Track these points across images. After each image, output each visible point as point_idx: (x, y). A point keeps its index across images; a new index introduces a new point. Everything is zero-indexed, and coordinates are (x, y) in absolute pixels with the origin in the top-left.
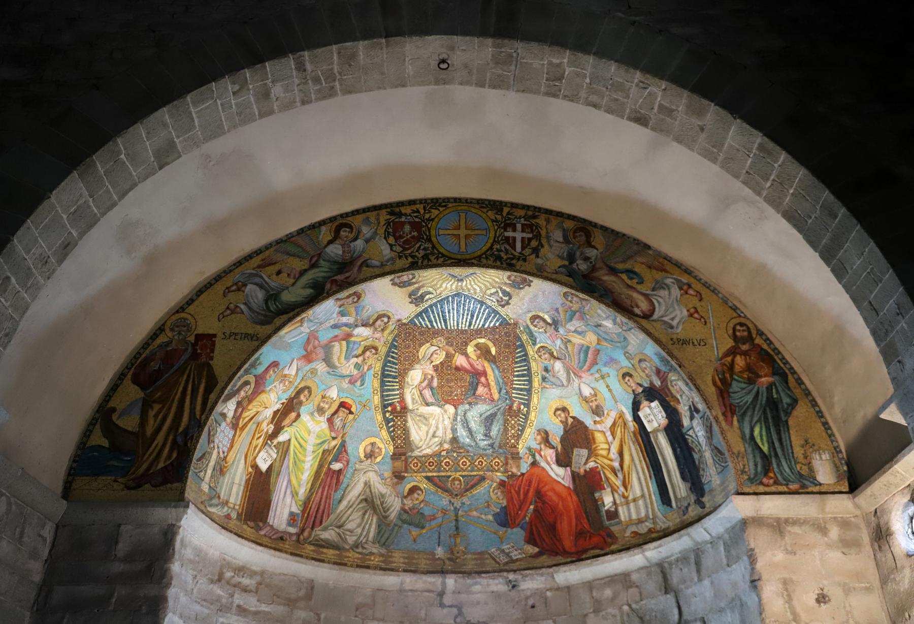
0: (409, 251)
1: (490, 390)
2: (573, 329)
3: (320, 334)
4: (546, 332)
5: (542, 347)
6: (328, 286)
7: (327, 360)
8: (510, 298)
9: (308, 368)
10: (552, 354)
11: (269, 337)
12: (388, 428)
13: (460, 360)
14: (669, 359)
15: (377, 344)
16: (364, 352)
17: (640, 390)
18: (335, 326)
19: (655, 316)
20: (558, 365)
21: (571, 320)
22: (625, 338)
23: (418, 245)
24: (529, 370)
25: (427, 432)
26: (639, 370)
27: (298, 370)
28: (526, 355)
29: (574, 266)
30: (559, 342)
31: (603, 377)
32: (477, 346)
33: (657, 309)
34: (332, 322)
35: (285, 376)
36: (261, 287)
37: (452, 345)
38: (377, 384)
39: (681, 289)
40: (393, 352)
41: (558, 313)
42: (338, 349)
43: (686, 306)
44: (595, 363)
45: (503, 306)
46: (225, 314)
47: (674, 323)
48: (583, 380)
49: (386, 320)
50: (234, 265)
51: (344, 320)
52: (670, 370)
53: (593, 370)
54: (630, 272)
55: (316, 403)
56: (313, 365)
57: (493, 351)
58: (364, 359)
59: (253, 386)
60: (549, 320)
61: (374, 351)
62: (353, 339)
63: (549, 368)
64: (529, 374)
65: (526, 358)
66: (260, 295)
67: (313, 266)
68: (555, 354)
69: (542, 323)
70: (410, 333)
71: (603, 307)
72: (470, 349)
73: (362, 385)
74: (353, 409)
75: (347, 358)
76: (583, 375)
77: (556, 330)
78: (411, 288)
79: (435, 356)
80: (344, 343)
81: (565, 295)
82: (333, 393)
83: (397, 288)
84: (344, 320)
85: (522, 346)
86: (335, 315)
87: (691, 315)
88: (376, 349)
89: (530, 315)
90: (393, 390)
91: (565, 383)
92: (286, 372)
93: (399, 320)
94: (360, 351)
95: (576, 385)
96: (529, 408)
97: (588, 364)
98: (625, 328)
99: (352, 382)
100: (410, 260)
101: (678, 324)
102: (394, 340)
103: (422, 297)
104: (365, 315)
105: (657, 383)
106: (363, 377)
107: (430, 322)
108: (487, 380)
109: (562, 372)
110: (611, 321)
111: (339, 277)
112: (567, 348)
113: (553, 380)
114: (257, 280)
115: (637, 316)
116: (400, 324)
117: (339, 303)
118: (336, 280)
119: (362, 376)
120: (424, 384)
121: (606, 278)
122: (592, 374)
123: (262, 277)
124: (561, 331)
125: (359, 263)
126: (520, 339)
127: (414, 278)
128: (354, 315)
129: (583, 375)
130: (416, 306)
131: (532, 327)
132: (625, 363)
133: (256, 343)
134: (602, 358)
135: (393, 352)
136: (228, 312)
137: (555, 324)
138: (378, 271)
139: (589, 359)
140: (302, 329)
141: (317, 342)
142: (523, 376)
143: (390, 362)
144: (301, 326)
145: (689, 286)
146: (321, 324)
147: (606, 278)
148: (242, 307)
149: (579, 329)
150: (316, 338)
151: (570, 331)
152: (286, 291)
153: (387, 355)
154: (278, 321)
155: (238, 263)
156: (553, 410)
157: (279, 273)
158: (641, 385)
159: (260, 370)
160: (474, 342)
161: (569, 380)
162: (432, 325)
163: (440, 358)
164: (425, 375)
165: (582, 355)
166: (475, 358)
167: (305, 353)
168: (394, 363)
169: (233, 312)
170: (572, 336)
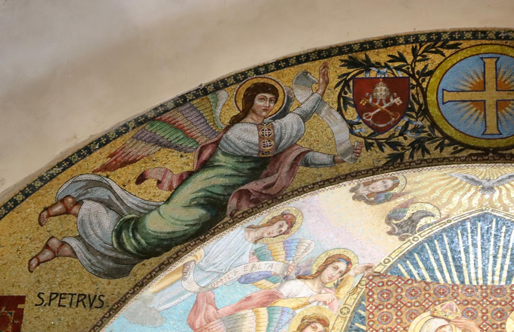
0: (386, 135)
6: (233, 203)
11: (123, 301)
15: (327, 313)
18: (246, 280)
23: (402, 123)
34: (241, 271)
36: (108, 205)
37: (473, 317)
46: (42, 258)
49: (342, 266)
50: (59, 165)
51: (264, 266)
61: (320, 327)
62: (280, 304)
66: (108, 221)
67: (205, 165)
78: (392, 205)
80: (263, 311)
83: (363, 205)
84: (264, 266)
86: (246, 258)
88: (324, 323)
93: (368, 268)
100: (388, 150)
102: (359, 305)
103: (412, 222)
104: (302, 257)
111: (252, 186)
114: (102, 193)
116: (372, 276)
117: (254, 234)
118: (247, 192)
123: (110, 188)
125: (290, 159)
127: (396, 185)
128: (282, 257)
130: (402, 239)
133: (99, 313)
136: (48, 254)
140: (185, 284)
141: (212, 309)
144: (183, 278)
146: (220, 274)
148: (74, 243)
150: (211, 302)
152: (155, 213)
155: (67, 163)
157: (141, 179)
169: (56, 254)
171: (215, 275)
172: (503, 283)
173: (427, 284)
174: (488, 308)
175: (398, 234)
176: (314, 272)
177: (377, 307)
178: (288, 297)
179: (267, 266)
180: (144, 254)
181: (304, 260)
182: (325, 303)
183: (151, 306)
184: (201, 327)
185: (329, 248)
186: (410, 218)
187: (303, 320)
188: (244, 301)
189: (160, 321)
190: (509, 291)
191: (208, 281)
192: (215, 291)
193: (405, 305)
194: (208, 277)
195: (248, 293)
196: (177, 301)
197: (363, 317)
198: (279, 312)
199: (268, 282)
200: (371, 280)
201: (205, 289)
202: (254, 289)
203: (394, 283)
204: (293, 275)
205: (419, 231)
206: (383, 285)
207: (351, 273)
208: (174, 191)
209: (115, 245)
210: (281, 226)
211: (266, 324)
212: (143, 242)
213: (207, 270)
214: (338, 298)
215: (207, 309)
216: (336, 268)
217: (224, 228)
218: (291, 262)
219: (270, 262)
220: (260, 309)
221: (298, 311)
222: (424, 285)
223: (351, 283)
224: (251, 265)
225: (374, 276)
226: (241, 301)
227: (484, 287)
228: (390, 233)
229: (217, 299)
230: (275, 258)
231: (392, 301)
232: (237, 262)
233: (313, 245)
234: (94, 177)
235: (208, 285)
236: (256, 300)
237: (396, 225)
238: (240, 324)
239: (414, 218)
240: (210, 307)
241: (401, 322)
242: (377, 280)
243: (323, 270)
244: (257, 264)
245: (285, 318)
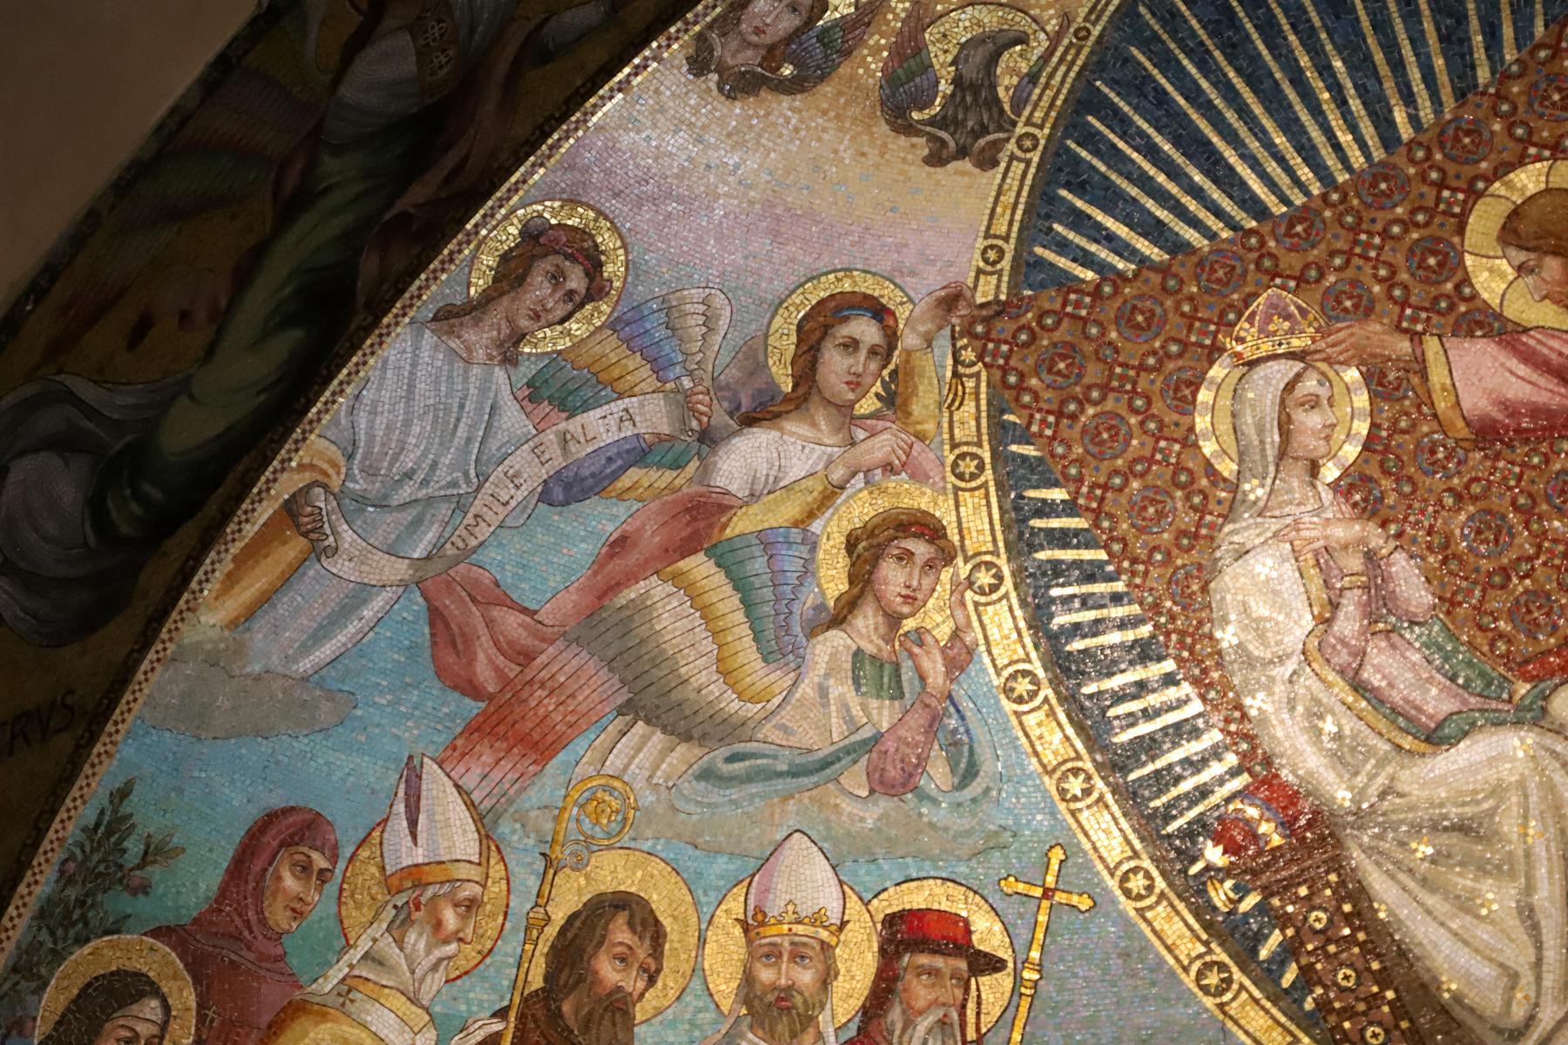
3: (498, 561)
7: (653, 700)
9: (548, 785)
11: (121, 679)
12: (1267, 976)
13: (1476, 377)
15: (921, 499)
16: (862, 578)
18: (569, 488)
25: (1528, 914)
27: (485, 823)
35: (415, 876)
37: (1366, 310)
38: (1054, 737)
40: (1045, 509)
42: (683, 617)
49: (866, 331)
51: (601, 427)
55: (725, 986)
56: (579, 758)
58: (894, 620)
59: (185, 997)
61: (921, 549)
62: (742, 524)
67: (290, 208)
70: (1068, 350)
72: (1492, 277)
73: (970, 773)
74: (987, 933)
75: (780, 648)
78: (871, 62)
79: (1311, 421)
80: (699, 566)
82: (808, 884)
84: (601, 427)
86: (513, 419)
90: (1180, 732)
92: (403, 852)
93: (950, 300)
94: (833, 580)
99: (893, 781)
102: (1000, 433)
103: (975, 90)
104: (718, 352)
106: (939, 720)
107: (1154, 230)
111: (419, 193)
114: (50, 421)
117: (480, 337)
118: (404, 217)
119: (934, 723)
120: (1348, 623)
125: (502, 67)
130: (987, 161)
133: (64, 742)
135: (1045, 509)
138: (596, 56)
140: (341, 566)
141: (512, 623)
143: (1057, 570)
144: (319, 549)
150: (495, 597)
152: (183, 401)
153: (1021, 542)
154: (153, 579)
157: (143, 326)
159: (193, 883)
160: (1484, 220)
162: (1177, 247)
163: (1345, 420)
164: (1325, 557)
167: (473, 707)
168: (1091, 573)
171: (444, 510)
172: (1378, 154)
173: (1164, 270)
174: (1387, 255)
175: (962, 153)
176: (787, 386)
177: (1060, 414)
178: (754, 496)
179: (612, 421)
180: (161, 525)
181: (725, 358)
182: (889, 468)
183: (257, 668)
184: (506, 682)
185: (779, 286)
186: (957, 82)
187: (851, 544)
188: (611, 556)
189: (326, 706)
191: (431, 535)
192: (491, 556)
193: (1142, 368)
194: (417, 522)
195: (610, 529)
196: (351, 629)
197: (1040, 460)
198: (757, 551)
199: (654, 474)
200: (987, 337)
201: (438, 565)
202: (622, 510)
203: (1060, 316)
204: (720, 418)
205: (1017, 107)
206: (1033, 337)
207: (909, 340)
208: (221, 319)
209: (92, 540)
210: (557, 277)
211: (735, 600)
212: (155, 493)
213: (396, 499)
214: (921, 437)
215: (490, 623)
216: (852, 345)
217: (355, 347)
218: (687, 383)
219: (617, 407)
220: (683, 565)
221: (816, 526)
222: (1156, 278)
223: (930, 371)
224: (550, 436)
225: (986, 321)
226: (600, 564)
227: (1335, 197)
228: (936, 159)
229: (507, 579)
230: (622, 386)
231: (1093, 373)
232: (493, 445)
233: (719, 300)
234: (29, 390)
235: (439, 546)
236: (652, 539)
237: (932, 122)
238: (643, 631)
239: (971, 72)
240: (497, 613)
241: (1161, 425)
242: (1004, 327)
243: (813, 365)
244: (574, 425)
245: (791, 565)
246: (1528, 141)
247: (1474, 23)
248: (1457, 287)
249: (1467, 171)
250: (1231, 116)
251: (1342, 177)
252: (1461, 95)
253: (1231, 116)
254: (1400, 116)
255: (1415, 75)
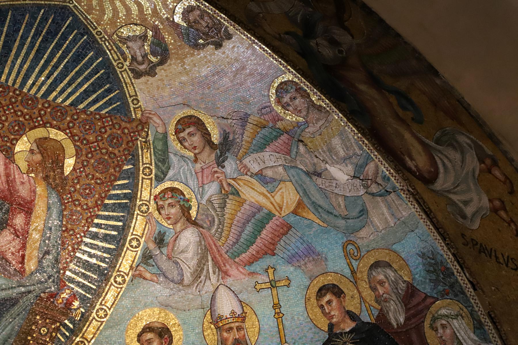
1: (24, 247)
2: (255, 168)
4: (196, 160)
5: (173, 190)
8: (162, 63)
10: (185, 210)
14: (455, 268)
17: (349, 326)
19: (439, 185)
20: (189, 238)
21: (261, 148)
22: (364, 212)
24: (123, 230)
26: (364, 286)
28: (132, 197)
29: (313, 43)
30: (212, 189)
31: (273, 285)
32: (42, 143)
33: (441, 176)
39: (481, 161)
41: (243, 126)
43: (487, 192)
44: (270, 250)
45: (138, 75)
47: (469, 211)
48: (229, 281)
52: (444, 295)
53: (257, 267)
54: (403, 97)
57: (69, 163)
60: (216, 138)
63: (169, 238)
64: (119, 239)
65: (127, 207)
68: (193, 213)
69: (197, 139)
71: (351, 131)
72: (23, 146)
76: (233, 271)
77: (220, 162)
81: (282, 88)
85: (133, 175)
87: (495, 210)
89: (180, 114)
91: (188, 278)
95: (209, 287)
96: (89, 311)
97: (253, 250)
98: (374, 189)
101: (474, 215)
105: (397, 316)
108: (28, 223)
109: (189, 254)
110: (350, 168)
112: (223, 206)
113: (165, 265)
115: (409, 170)
121: (363, 87)
122: (252, 274)
124: (230, 166)
126: (135, 159)
129: (233, 271)
131: (172, 138)
132: (337, 264)
134: (292, 243)
137: (225, 148)
139: (261, 240)
142: (106, 238)
145: (495, 163)
147: (363, 87)
149: (269, 173)
151: (246, 171)
156: (139, 330)
158: (352, 316)
160: (39, 133)
161: (197, 275)
165: (249, 228)
166: (23, 165)
170: (247, 183)
172: (39, 95)
174: (10, 116)
190: (40, 106)
227: (18, 92)
246: (69, 128)
247: (94, 96)
248: (13, 139)
249: (51, 120)
250: (24, 51)
251: (25, 90)
252: (71, 104)
253: (24, 51)
254: (54, 94)
255: (69, 90)
